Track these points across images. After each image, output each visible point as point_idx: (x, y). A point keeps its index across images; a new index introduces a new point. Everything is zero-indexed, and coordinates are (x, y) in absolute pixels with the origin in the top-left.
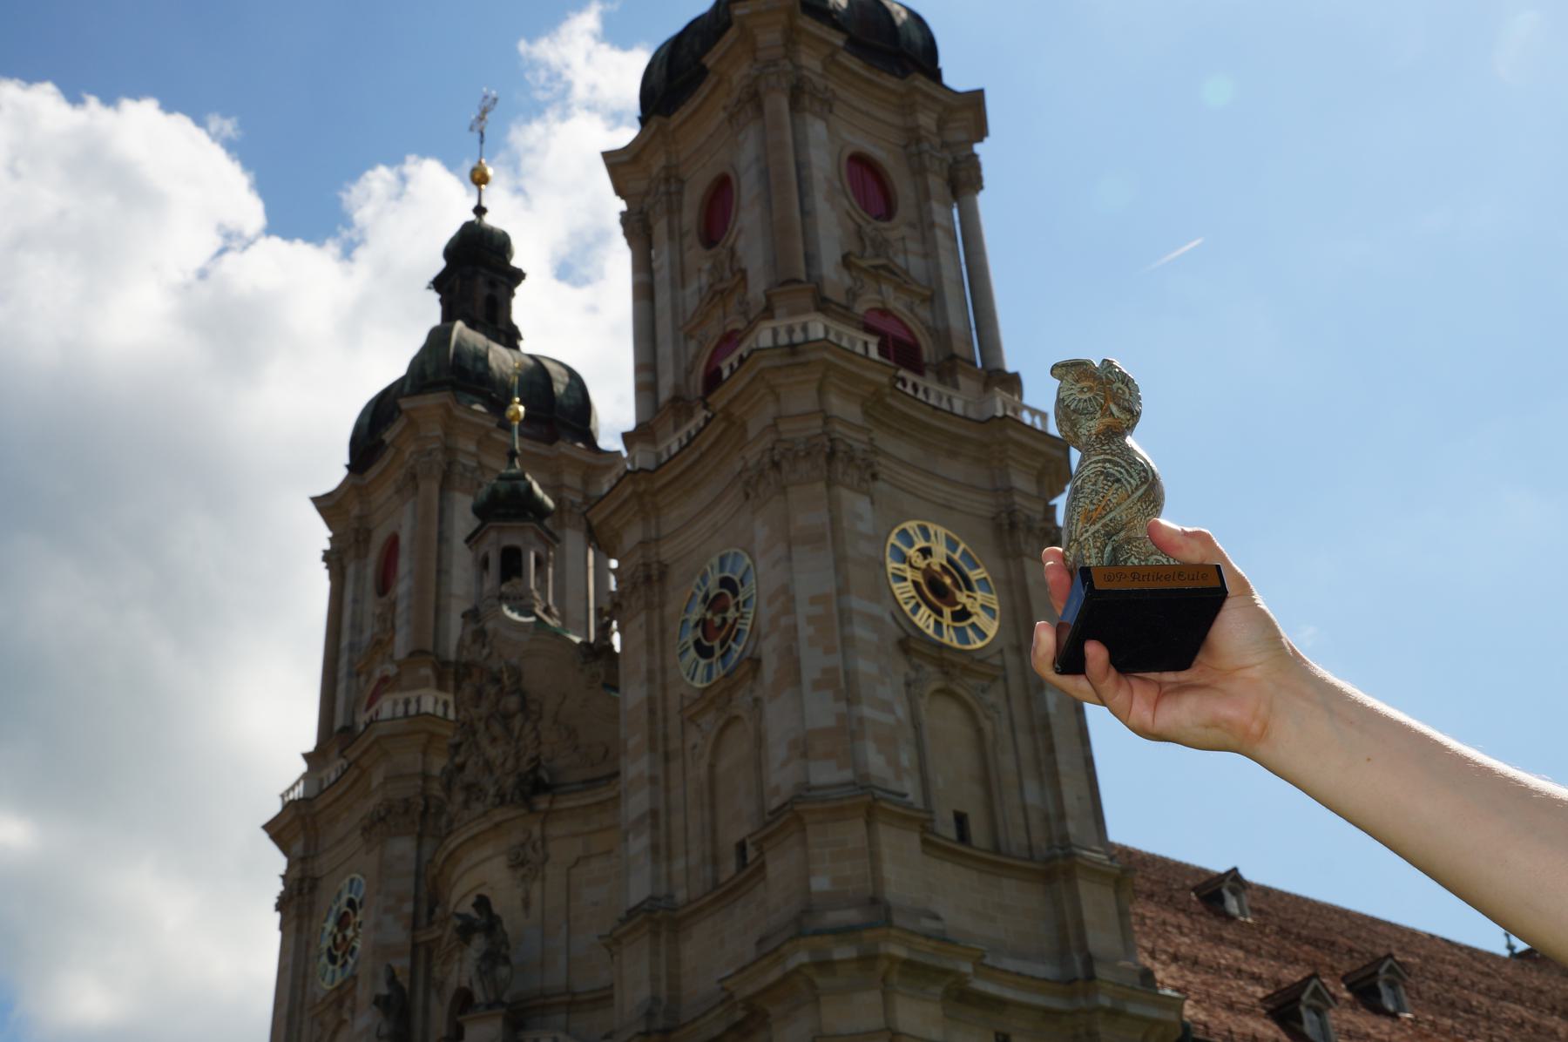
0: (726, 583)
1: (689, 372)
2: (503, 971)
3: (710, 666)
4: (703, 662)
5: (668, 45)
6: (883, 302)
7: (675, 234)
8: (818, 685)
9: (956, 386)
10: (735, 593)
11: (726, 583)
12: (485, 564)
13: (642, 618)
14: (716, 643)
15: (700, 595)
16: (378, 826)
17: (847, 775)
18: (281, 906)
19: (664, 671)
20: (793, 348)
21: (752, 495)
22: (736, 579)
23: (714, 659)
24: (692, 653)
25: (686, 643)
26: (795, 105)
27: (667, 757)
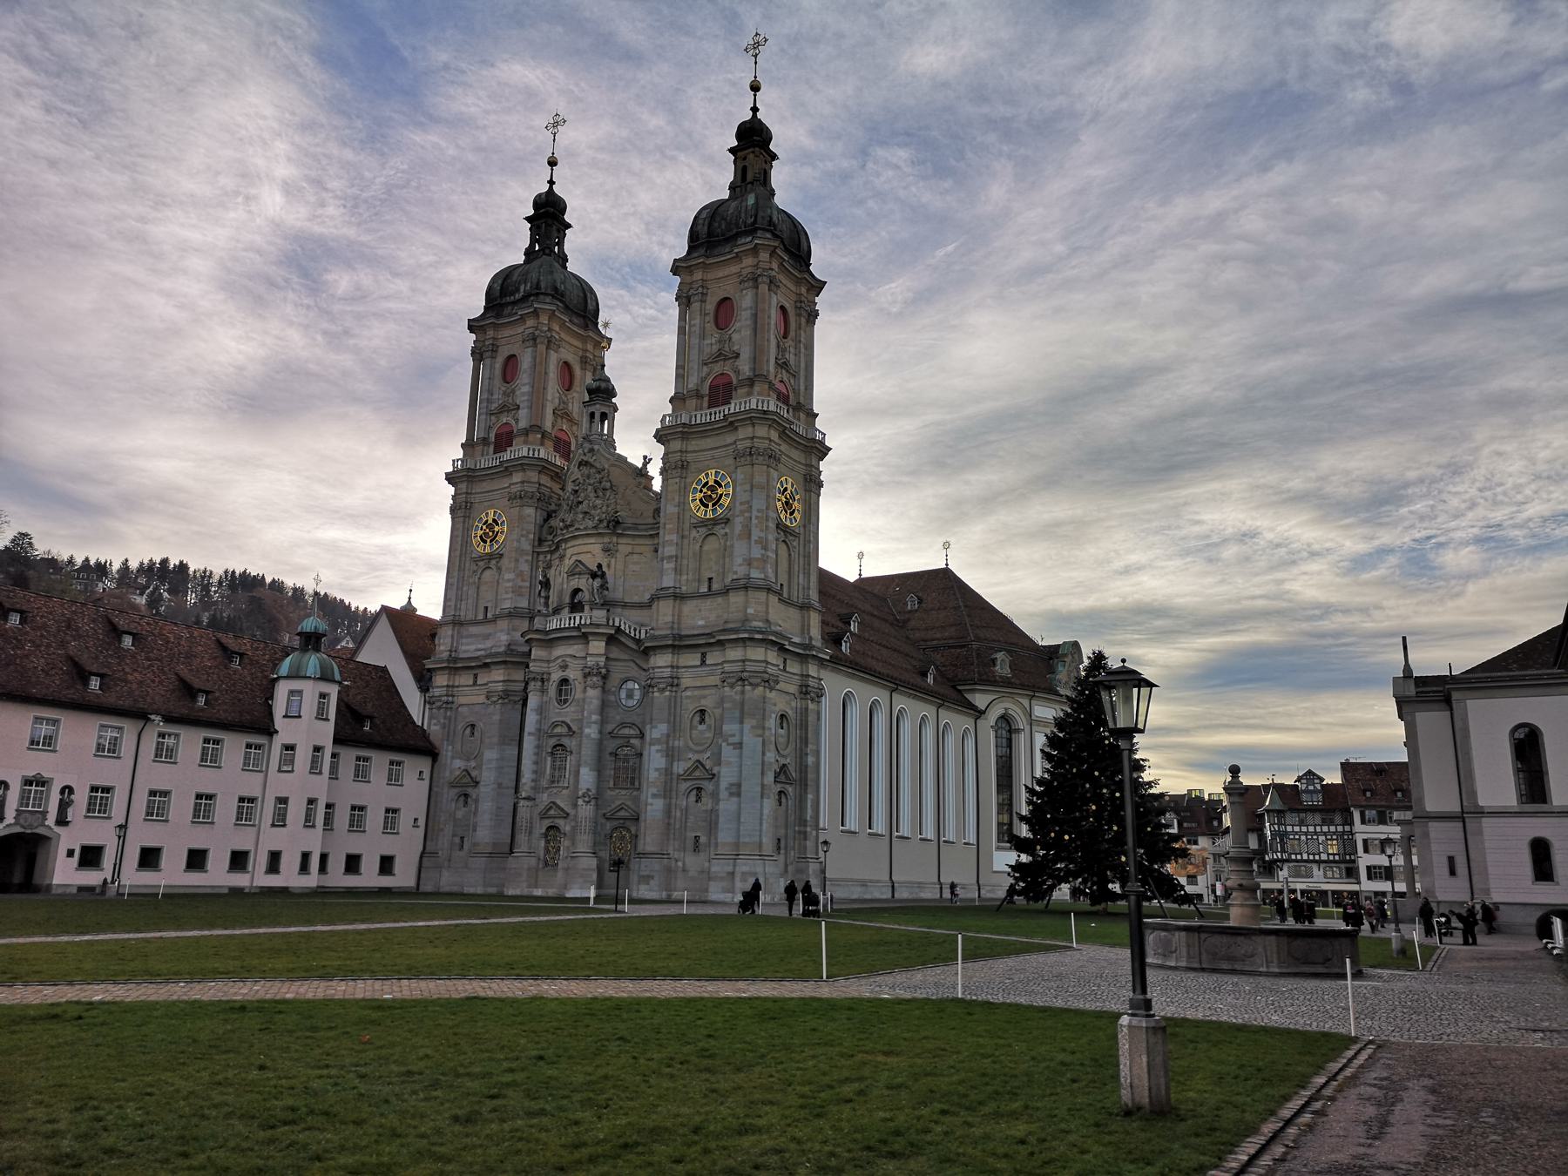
1: (703, 380)
2: (606, 592)
5: (705, 212)
7: (704, 314)
8: (756, 542)
12: (592, 415)
13: (677, 480)
15: (704, 481)
16: (518, 498)
17: (762, 576)
18: (453, 510)
19: (684, 503)
20: (765, 412)
27: (683, 537)
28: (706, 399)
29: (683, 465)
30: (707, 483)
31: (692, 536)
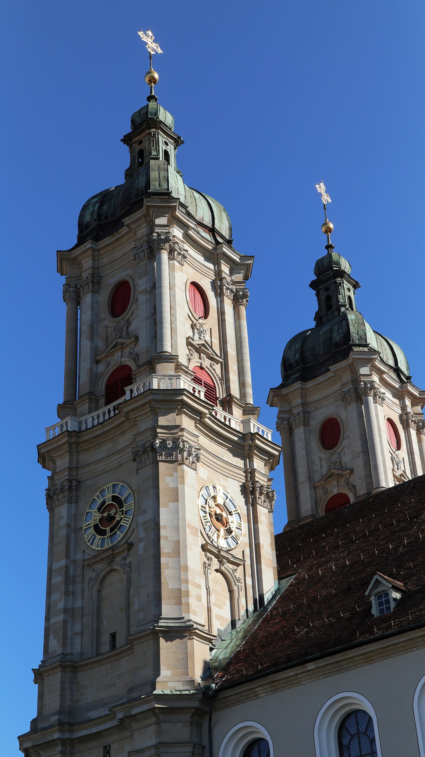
0: (114, 498)
3: (103, 540)
4: (98, 537)
6: (201, 364)
9: (231, 413)
10: (121, 506)
11: (114, 498)
14: (108, 529)
15: (99, 502)
21: (138, 459)
22: (123, 499)
23: (106, 537)
24: (92, 530)
25: (89, 524)
26: (171, 257)
28: (102, 401)
29: (70, 487)
30: (104, 503)
31: (87, 578)
